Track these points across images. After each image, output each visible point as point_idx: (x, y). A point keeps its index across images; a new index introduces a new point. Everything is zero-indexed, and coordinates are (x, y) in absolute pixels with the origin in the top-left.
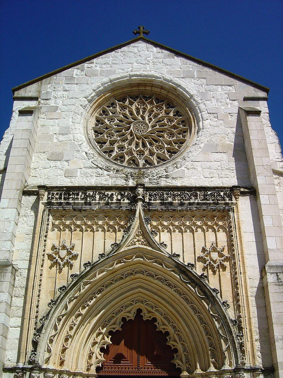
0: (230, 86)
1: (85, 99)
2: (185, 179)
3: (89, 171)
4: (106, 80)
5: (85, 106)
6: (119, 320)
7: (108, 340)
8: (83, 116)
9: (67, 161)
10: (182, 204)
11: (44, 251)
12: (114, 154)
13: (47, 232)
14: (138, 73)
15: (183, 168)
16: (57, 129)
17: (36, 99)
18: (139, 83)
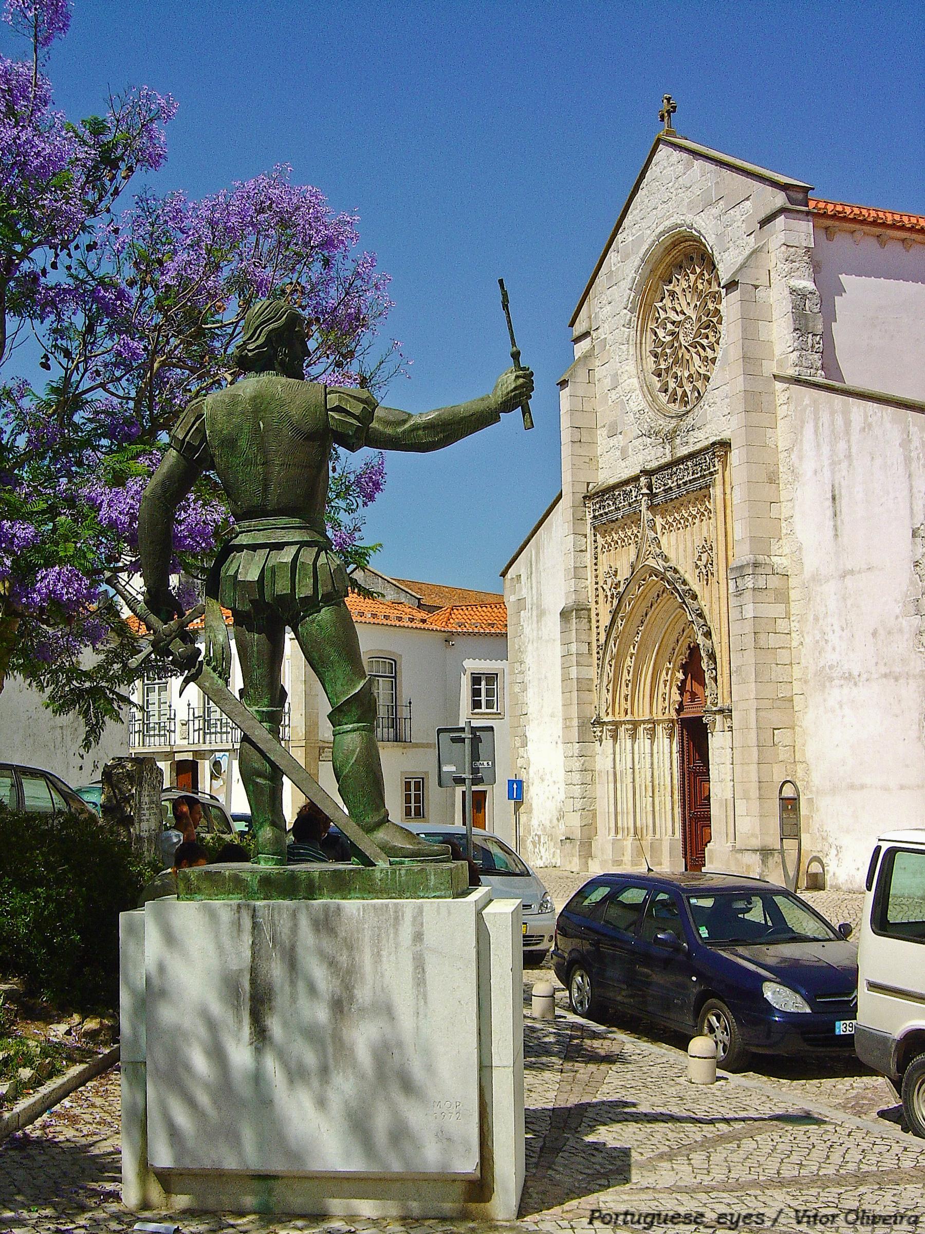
0: (747, 199)
1: (625, 311)
2: (708, 426)
3: (636, 443)
4: (637, 262)
5: (629, 324)
6: (684, 649)
7: (681, 676)
8: (631, 342)
9: (621, 433)
10: (679, 486)
11: (597, 583)
12: (670, 390)
13: (596, 558)
14: (661, 229)
15: (706, 407)
16: (607, 383)
17: (586, 334)
18: (672, 243)
